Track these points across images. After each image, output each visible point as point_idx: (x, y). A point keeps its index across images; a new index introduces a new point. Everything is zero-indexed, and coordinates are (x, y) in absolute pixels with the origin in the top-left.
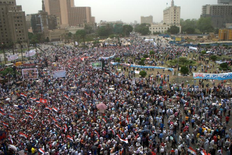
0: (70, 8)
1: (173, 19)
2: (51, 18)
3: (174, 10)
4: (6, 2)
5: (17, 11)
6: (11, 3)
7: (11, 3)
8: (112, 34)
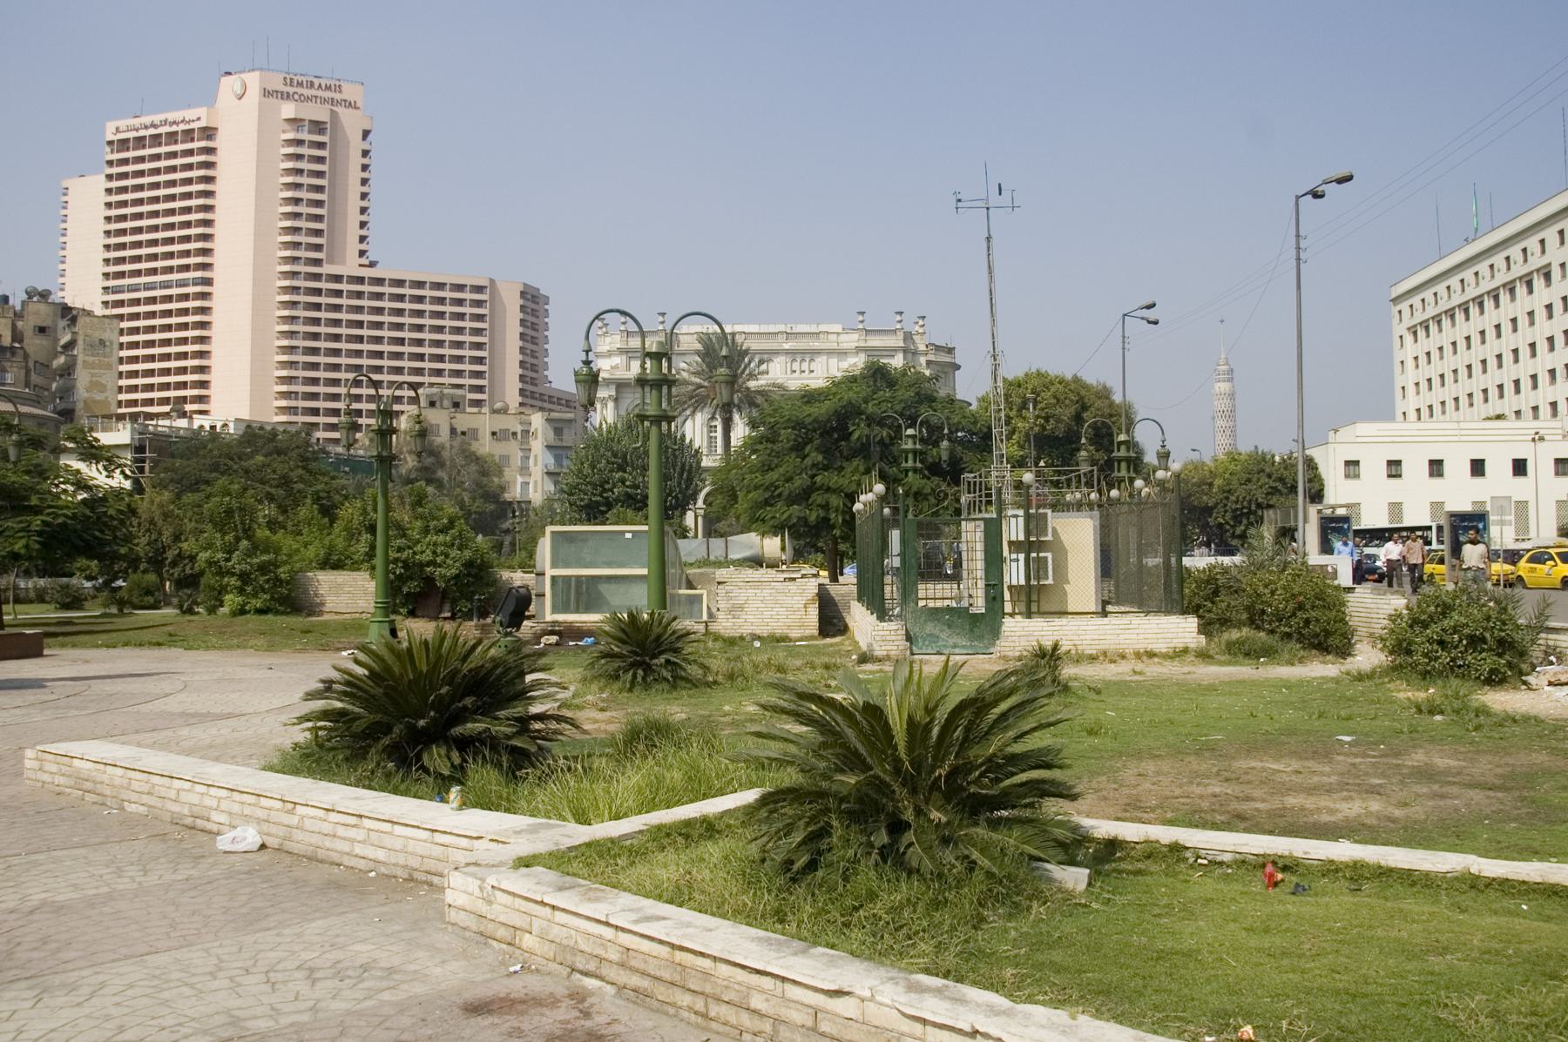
2: (17, 336)
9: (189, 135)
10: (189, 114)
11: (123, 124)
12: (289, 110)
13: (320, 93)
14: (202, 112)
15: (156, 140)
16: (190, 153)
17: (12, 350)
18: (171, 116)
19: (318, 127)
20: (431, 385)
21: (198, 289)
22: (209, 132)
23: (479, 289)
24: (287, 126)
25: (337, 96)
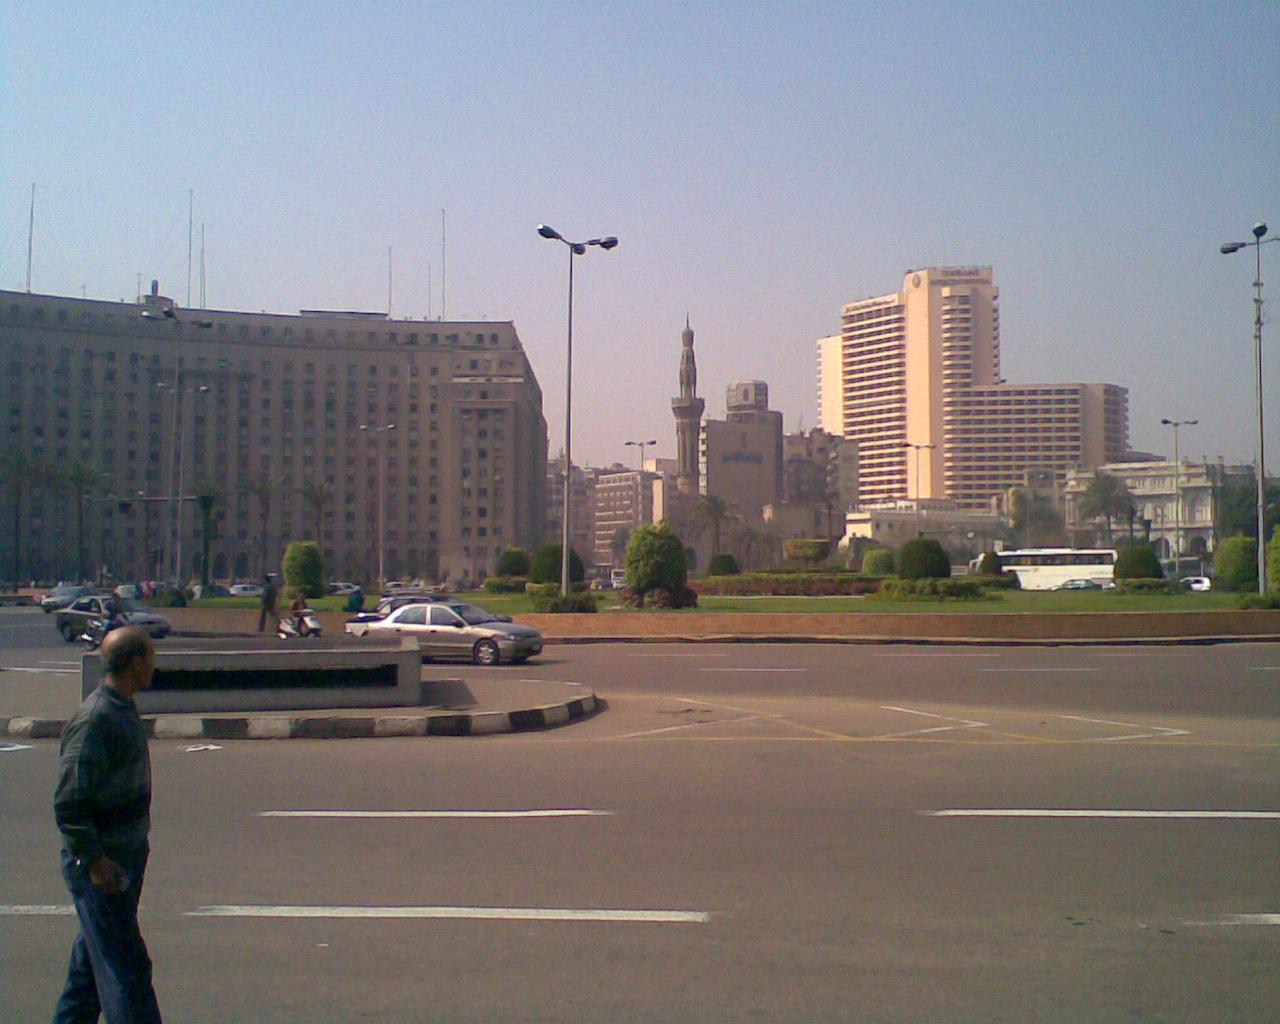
2: (810, 454)
4: (461, 336)
5: (495, 380)
6: (487, 340)
7: (487, 340)
9: (888, 311)
10: (888, 298)
11: (850, 306)
12: (946, 292)
13: (964, 277)
14: (895, 297)
15: (870, 315)
16: (888, 322)
18: (878, 300)
19: (964, 299)
20: (1031, 466)
21: (898, 405)
22: (900, 308)
23: (1074, 392)
24: (946, 301)
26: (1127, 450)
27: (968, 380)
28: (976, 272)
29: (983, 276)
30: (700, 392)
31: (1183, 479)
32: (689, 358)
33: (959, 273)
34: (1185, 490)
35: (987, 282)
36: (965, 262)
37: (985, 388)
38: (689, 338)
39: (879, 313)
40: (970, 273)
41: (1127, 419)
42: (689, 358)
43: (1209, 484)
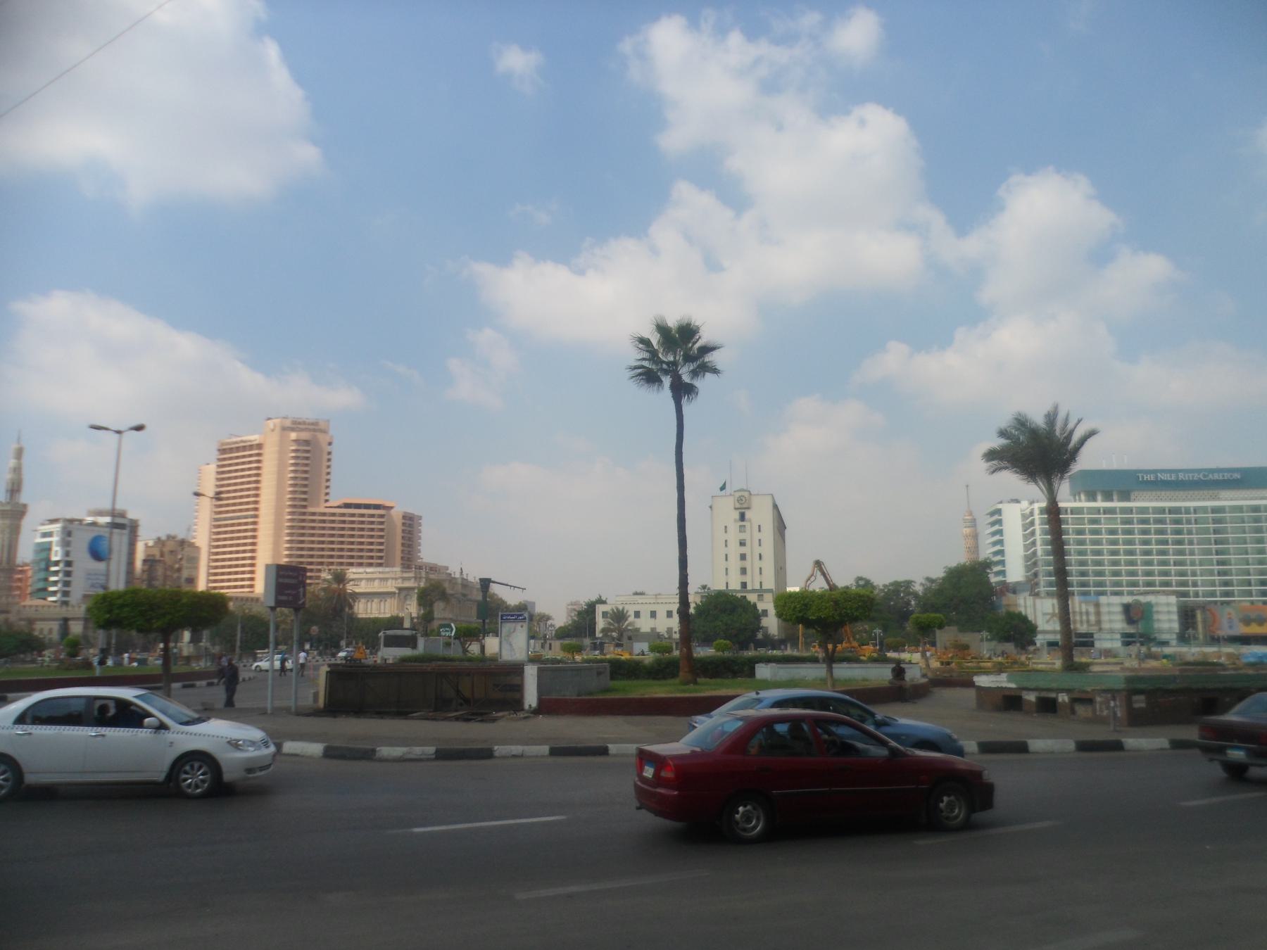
0: (304, 514)
1: (735, 564)
2: (162, 555)
3: (736, 515)
8: (347, 637)
9: (251, 447)
12: (293, 436)
13: (307, 426)
16: (251, 456)
17: (159, 561)
18: (244, 438)
19: (307, 442)
22: (260, 446)
24: (292, 443)
25: (316, 427)
26: (420, 560)
27: (304, 503)
28: (316, 424)
29: (322, 426)
30: (24, 498)
31: (400, 581)
32: (17, 470)
33: (304, 423)
34: (400, 589)
35: (324, 432)
36: (308, 415)
37: (322, 510)
38: (19, 453)
39: (244, 449)
40: (313, 424)
41: (420, 538)
42: (17, 470)
43: (416, 585)
